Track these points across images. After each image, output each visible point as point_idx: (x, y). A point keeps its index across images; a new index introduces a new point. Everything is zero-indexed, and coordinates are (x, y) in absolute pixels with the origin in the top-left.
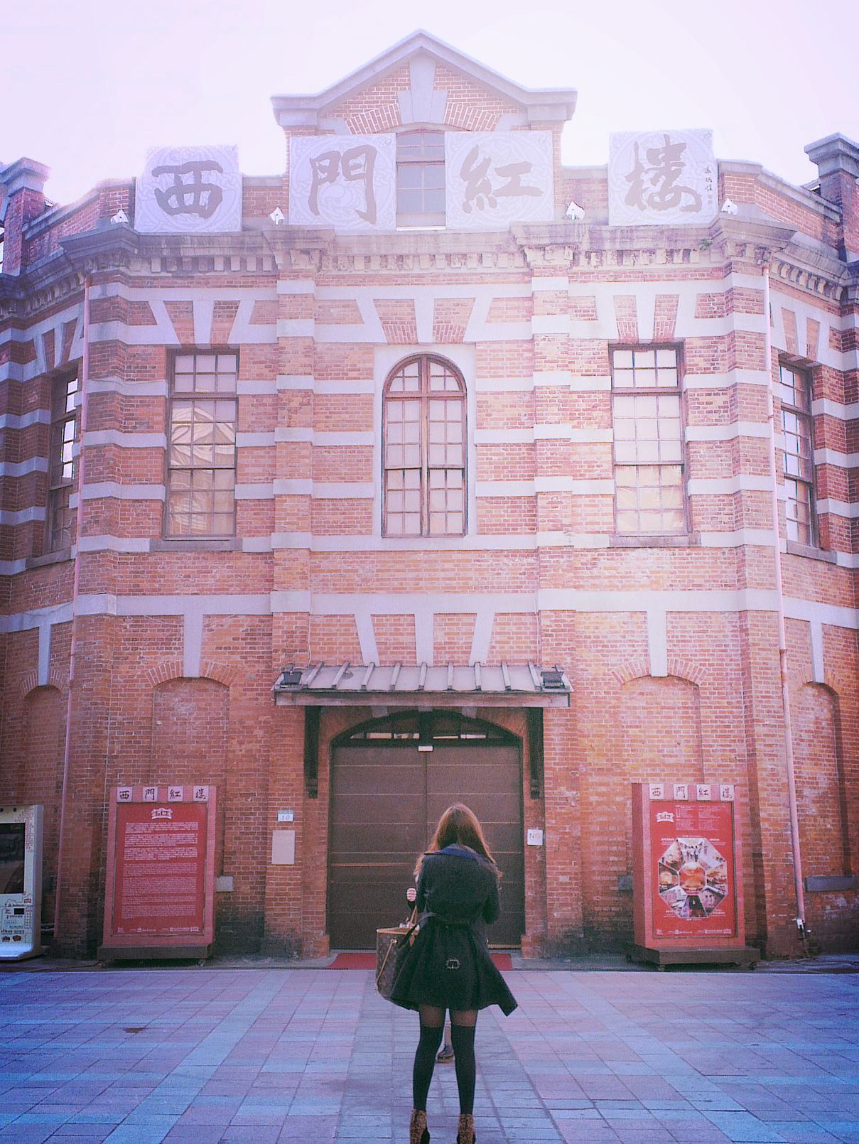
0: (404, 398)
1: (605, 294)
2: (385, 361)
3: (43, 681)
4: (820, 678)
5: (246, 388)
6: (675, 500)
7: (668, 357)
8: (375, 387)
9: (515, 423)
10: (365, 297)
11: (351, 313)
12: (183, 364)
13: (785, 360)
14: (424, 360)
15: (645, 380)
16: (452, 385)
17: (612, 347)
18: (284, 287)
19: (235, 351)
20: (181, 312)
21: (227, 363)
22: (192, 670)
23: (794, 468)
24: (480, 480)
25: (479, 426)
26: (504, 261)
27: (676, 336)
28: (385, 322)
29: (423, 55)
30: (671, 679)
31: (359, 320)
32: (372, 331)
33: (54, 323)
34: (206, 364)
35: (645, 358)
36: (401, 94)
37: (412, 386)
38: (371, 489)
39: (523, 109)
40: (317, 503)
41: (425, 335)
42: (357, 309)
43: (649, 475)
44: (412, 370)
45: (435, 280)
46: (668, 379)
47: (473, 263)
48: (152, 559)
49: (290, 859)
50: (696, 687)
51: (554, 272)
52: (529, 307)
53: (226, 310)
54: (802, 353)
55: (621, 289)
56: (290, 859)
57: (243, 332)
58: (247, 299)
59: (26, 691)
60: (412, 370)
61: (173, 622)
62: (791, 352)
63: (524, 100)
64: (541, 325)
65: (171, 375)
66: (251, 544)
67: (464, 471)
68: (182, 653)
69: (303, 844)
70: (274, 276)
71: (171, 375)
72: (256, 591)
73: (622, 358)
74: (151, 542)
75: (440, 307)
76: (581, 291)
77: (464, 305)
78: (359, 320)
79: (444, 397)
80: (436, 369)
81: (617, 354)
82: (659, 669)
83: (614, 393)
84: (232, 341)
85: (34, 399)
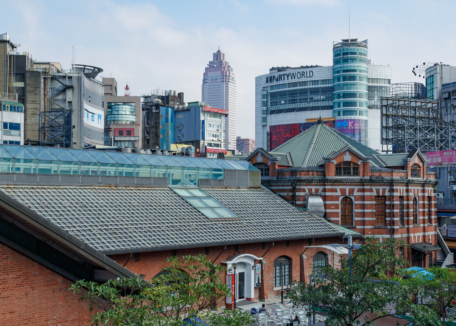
1: (374, 188)
2: (341, 198)
8: (339, 202)
9: (361, 208)
10: (338, 188)
11: (335, 191)
14: (346, 198)
18: (327, 187)
32: (339, 193)
41: (347, 194)
45: (348, 185)
51: (367, 185)
52: (363, 191)
55: (377, 187)
60: (344, 199)
64: (367, 194)
67: (352, 215)
70: (325, 185)
75: (349, 189)
77: (354, 190)
80: (348, 199)
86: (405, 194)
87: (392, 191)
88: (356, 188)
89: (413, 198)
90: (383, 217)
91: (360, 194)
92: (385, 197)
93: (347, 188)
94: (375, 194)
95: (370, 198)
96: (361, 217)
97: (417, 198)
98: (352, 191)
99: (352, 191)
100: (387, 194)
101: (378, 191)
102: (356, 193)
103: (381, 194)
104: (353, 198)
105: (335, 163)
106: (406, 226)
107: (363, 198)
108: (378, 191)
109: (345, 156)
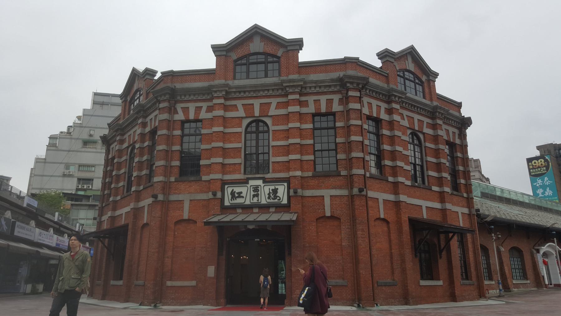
0: (251, 133)
1: (311, 99)
2: (245, 122)
3: (145, 222)
4: (382, 216)
5: (204, 131)
6: (333, 160)
7: (331, 118)
8: (241, 130)
10: (239, 103)
11: (235, 108)
12: (187, 125)
13: (369, 118)
14: (257, 121)
15: (324, 125)
16: (266, 128)
17: (314, 115)
19: (201, 121)
20: (186, 110)
21: (199, 124)
22: (186, 216)
23: (373, 151)
24: (273, 156)
25: (273, 141)
26: (280, 91)
27: (333, 111)
28: (245, 110)
29: (256, 33)
30: (332, 217)
31: (238, 110)
32: (241, 113)
33: (152, 116)
34: (193, 125)
35: (324, 119)
36: (251, 45)
37: (254, 129)
38: (240, 160)
39: (286, 47)
40: (223, 165)
41: (257, 113)
42: (237, 107)
43: (325, 154)
44: (254, 124)
46: (331, 124)
47: (271, 92)
48: (175, 183)
49: (213, 276)
50: (339, 219)
53: (198, 109)
54: (375, 115)
55: (316, 98)
56: (213, 276)
57: (203, 115)
58: (205, 105)
59: (141, 225)
61: (181, 202)
62: (371, 115)
63: (287, 44)
64: (291, 109)
65: (182, 129)
66: (204, 178)
67: (269, 154)
68: (183, 212)
69: (217, 270)
71: (182, 129)
72: (205, 192)
73: (317, 118)
74: (175, 179)
76: (303, 98)
78: (238, 110)
79: (264, 132)
80: (261, 124)
81: (316, 118)
82: (328, 214)
83: (314, 129)
84: (200, 118)
85: (147, 137)
86: (384, 116)
87: (345, 100)
88: (274, 102)
89: (409, 132)
90: (333, 153)
91: (282, 112)
92: (334, 114)
93: (256, 103)
94: (311, 109)
95: (301, 117)
96: (283, 156)
97: (421, 136)
98: (265, 107)
99: (265, 107)
100: (336, 107)
101: (317, 102)
102: (273, 111)
103: (323, 110)
104: (269, 121)
105: (235, 57)
106: (391, 179)
107: (287, 118)
108: (317, 102)
109: (251, 45)
